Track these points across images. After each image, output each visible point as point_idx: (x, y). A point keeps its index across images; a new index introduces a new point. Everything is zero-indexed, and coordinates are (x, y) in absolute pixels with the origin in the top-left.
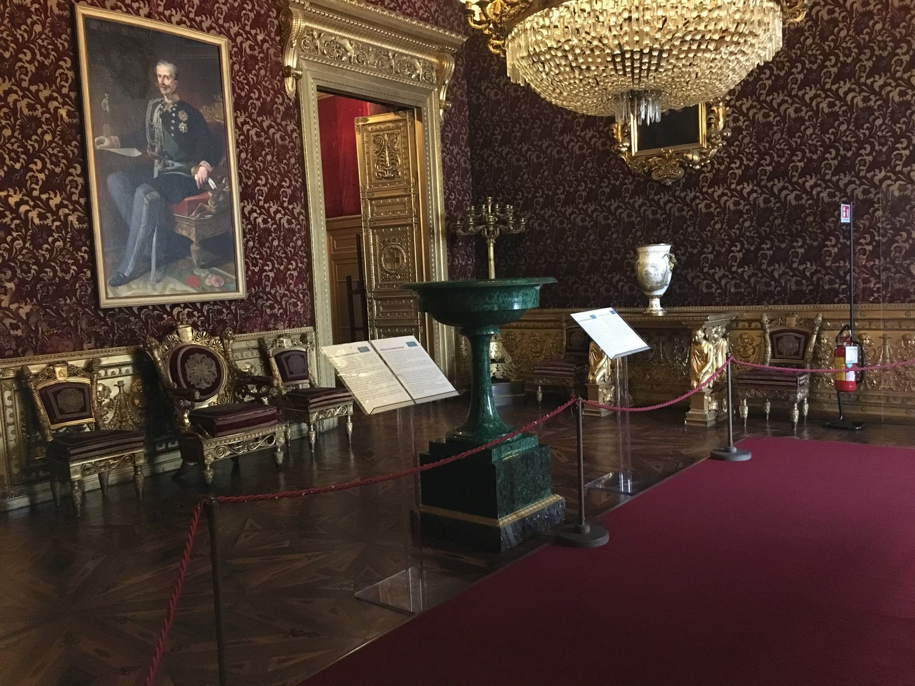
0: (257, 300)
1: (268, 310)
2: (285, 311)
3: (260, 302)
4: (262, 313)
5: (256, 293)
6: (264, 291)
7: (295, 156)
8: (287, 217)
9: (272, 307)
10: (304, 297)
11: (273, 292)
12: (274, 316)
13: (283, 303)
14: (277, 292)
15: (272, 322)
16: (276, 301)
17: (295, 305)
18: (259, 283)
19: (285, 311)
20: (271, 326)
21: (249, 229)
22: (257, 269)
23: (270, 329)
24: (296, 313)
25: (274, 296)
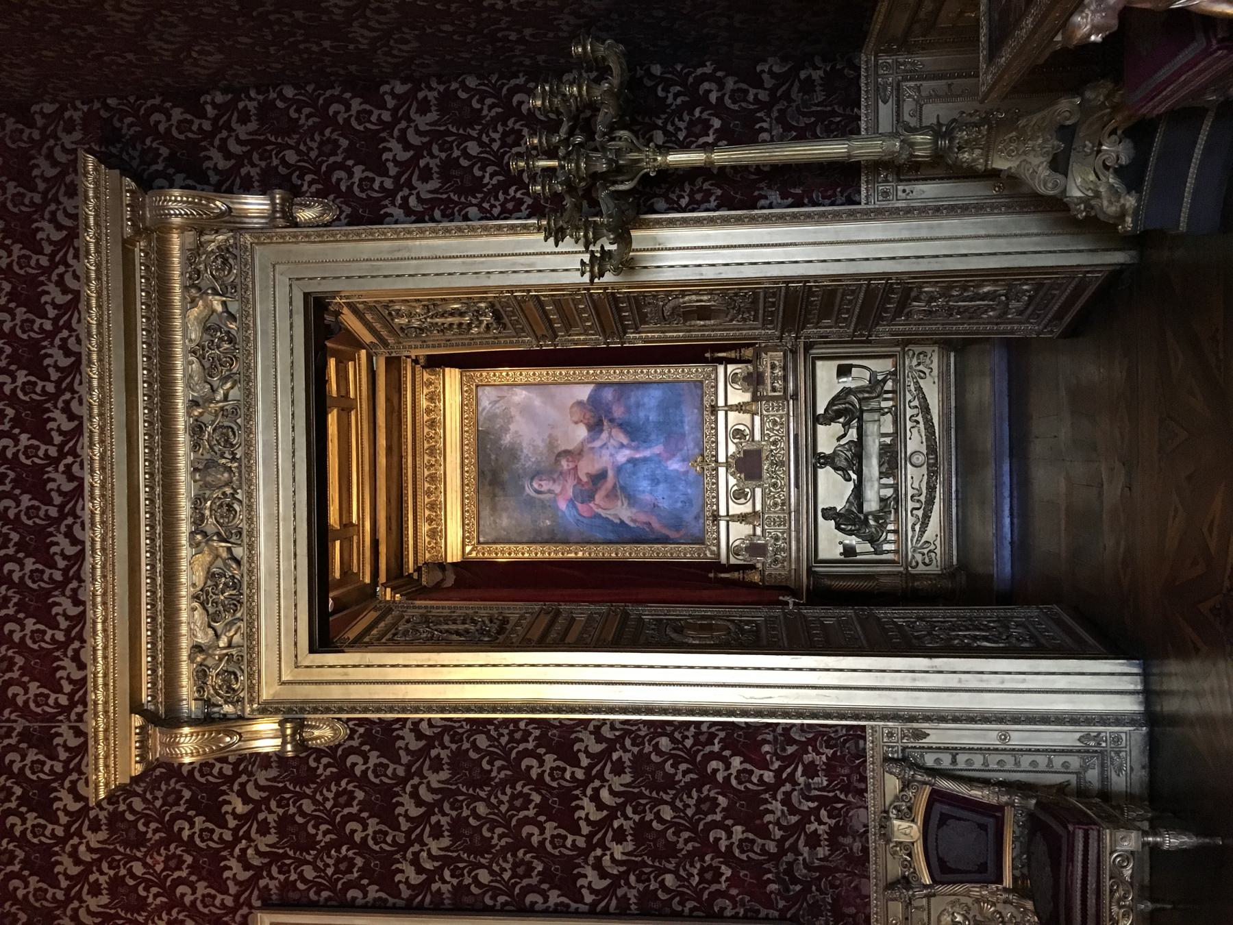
0: (795, 881)
1: (822, 852)
2: (824, 802)
3: (800, 872)
4: (825, 871)
5: (778, 880)
6: (775, 858)
7: (472, 733)
8: (607, 775)
9: (813, 841)
10: (792, 741)
11: (778, 834)
12: (836, 833)
13: (806, 806)
14: (778, 823)
15: (848, 840)
16: (800, 826)
17: (811, 771)
18: (756, 868)
19: (824, 802)
20: (857, 846)
21: (638, 881)
22: (727, 872)
23: (865, 850)
24: (830, 770)
25: (790, 830)
